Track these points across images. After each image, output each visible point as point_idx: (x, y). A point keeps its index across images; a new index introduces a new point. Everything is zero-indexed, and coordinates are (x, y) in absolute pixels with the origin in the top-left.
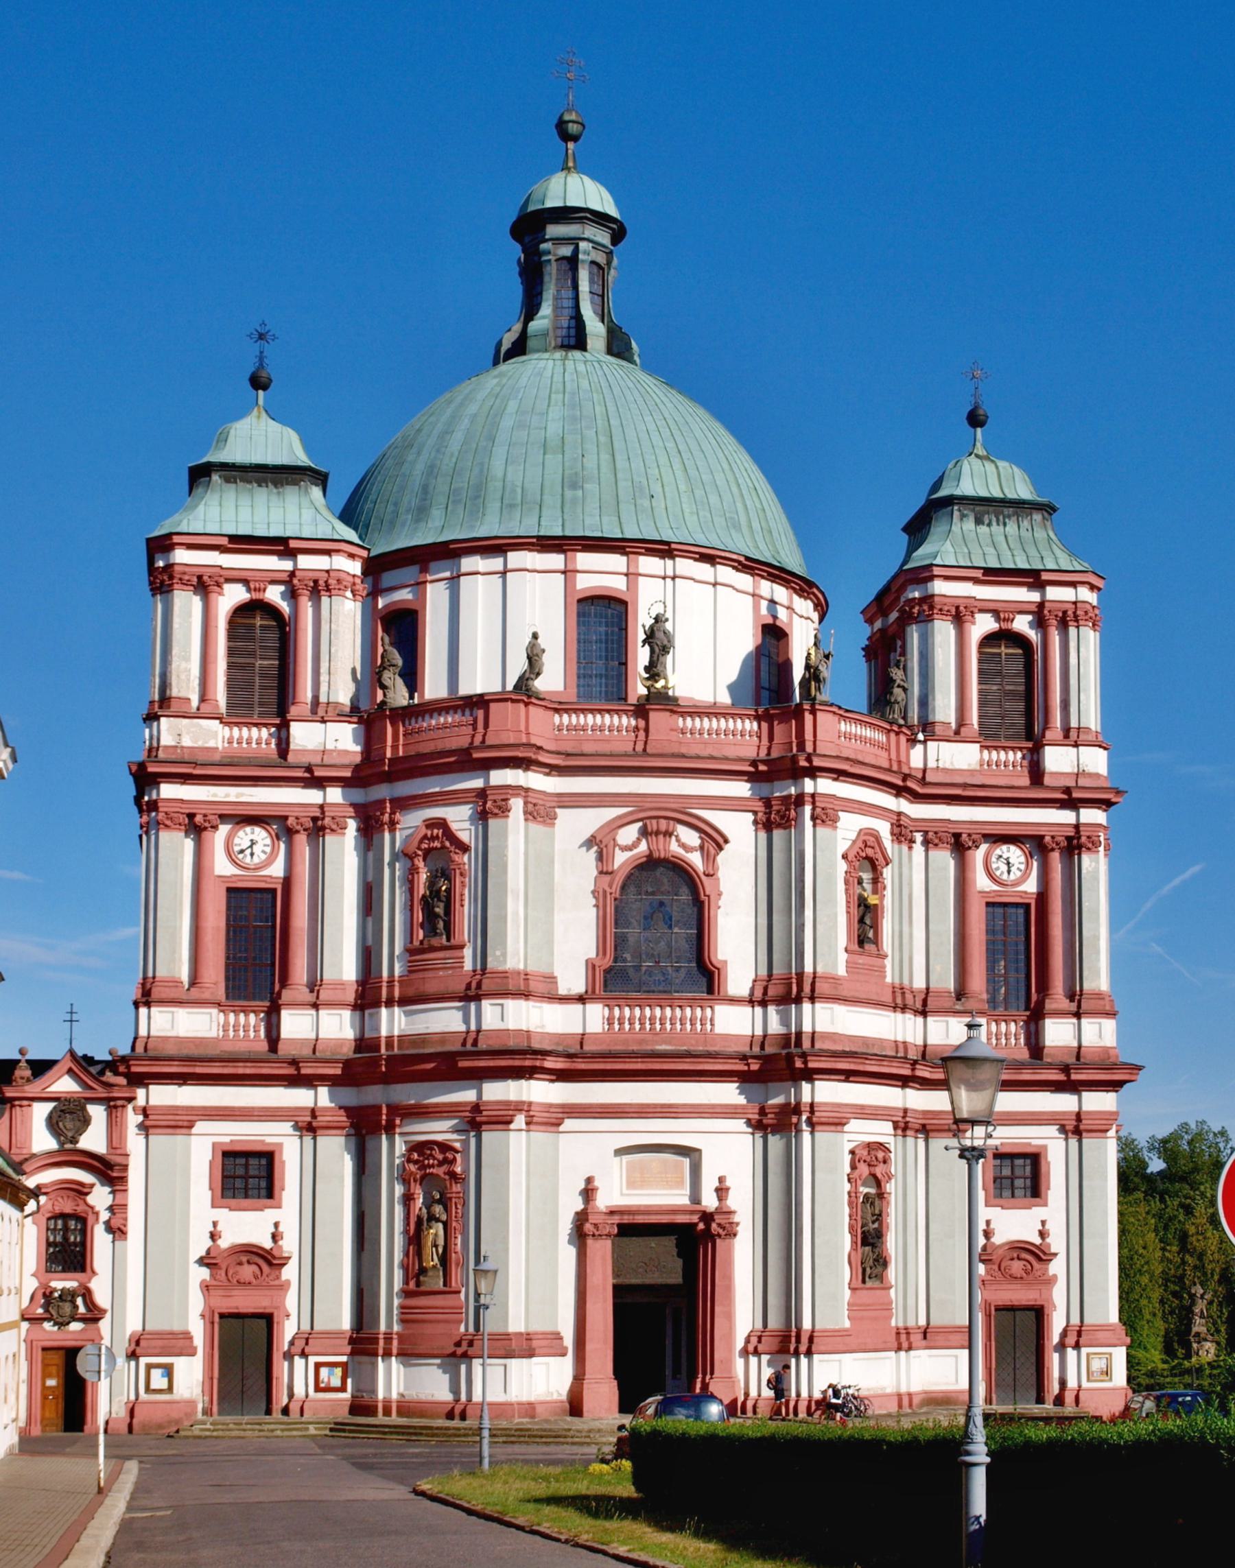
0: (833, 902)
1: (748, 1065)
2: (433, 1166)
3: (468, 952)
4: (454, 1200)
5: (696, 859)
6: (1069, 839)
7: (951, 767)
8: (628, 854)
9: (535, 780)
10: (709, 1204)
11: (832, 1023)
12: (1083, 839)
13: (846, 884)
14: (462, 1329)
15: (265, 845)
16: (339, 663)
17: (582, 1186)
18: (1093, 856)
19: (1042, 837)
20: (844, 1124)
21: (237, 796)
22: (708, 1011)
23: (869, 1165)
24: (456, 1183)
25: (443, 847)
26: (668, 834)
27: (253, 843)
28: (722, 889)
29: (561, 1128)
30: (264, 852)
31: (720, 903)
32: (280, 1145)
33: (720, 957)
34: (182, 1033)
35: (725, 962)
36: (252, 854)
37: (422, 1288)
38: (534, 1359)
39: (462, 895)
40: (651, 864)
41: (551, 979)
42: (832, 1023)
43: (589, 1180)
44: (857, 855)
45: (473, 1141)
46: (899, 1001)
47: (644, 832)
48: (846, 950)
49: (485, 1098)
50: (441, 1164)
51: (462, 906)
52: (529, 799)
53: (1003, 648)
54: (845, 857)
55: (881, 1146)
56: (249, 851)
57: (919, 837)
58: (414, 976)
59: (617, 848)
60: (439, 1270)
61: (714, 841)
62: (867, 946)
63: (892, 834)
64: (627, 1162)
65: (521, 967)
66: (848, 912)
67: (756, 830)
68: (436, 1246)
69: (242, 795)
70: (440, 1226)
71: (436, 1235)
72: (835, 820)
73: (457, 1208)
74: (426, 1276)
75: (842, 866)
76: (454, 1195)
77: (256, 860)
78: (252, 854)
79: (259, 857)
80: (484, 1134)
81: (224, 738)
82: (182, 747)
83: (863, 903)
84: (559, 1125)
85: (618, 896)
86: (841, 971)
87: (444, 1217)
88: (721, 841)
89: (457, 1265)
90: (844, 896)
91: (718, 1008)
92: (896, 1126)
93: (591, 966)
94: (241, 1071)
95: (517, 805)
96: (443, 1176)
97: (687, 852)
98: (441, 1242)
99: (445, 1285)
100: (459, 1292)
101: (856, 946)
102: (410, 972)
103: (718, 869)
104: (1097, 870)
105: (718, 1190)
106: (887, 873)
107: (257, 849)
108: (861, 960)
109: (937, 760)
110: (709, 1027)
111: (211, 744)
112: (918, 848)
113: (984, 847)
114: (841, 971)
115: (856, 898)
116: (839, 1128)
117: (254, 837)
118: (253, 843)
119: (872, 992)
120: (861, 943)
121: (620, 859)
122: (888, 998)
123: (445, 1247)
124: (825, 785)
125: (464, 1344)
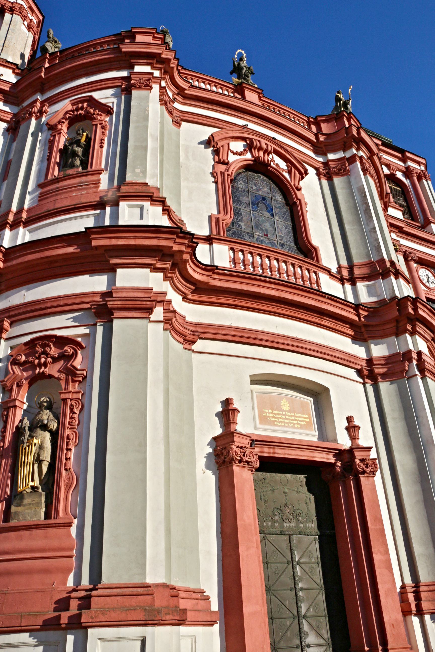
1: (358, 315)
2: (45, 364)
4: (69, 403)
8: (237, 157)
10: (344, 443)
14: (70, 583)
17: (219, 409)
24: (74, 381)
25: (88, 112)
37: (13, 523)
38: (183, 629)
39: (102, 140)
43: (227, 403)
45: (100, 330)
49: (119, 284)
50: (55, 360)
51: (102, 147)
58: (42, 202)
60: (41, 495)
67: (320, 179)
68: (39, 461)
70: (47, 435)
71: (41, 447)
73: (72, 412)
74: (19, 505)
76: (70, 396)
80: (116, 323)
84: (193, 342)
87: (54, 425)
89: (68, 487)
96: (57, 375)
98: (47, 456)
99: (47, 516)
100: (69, 525)
102: (39, 201)
105: (347, 429)
123: (52, 466)
125: (74, 604)
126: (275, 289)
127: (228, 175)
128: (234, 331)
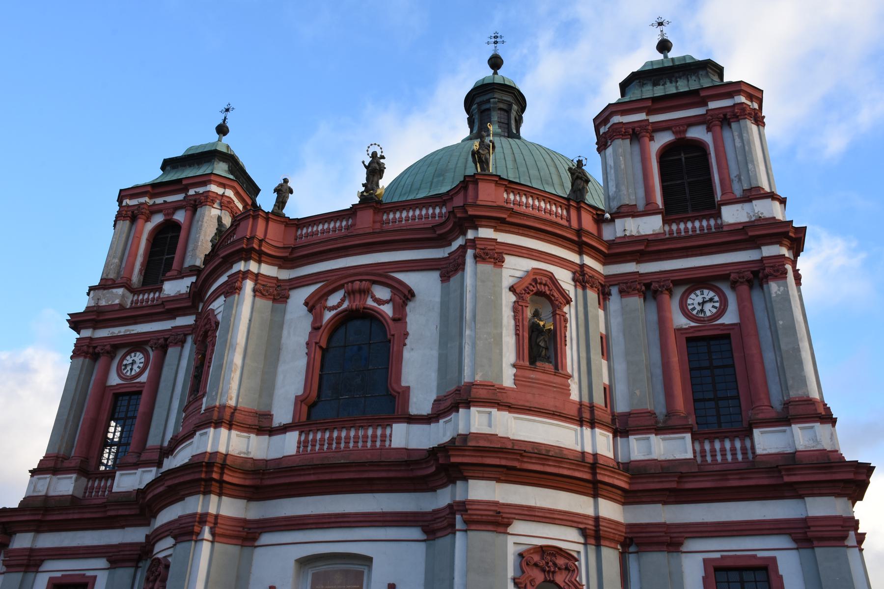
0: (498, 324)
3: (204, 400)
5: (388, 310)
6: (755, 274)
7: (637, 235)
8: (333, 312)
9: (268, 270)
11: (490, 425)
12: (767, 270)
13: (514, 312)
15: (140, 363)
16: (200, 243)
18: (781, 282)
19: (728, 275)
20: (508, 525)
21: (126, 331)
22: (388, 431)
23: (543, 571)
26: (366, 292)
27: (134, 362)
28: (408, 330)
29: (257, 544)
30: (139, 367)
31: (407, 341)
32: (95, 577)
33: (404, 384)
34: (52, 493)
35: (408, 388)
36: (131, 369)
39: (211, 359)
40: (346, 318)
41: (269, 416)
42: (490, 425)
44: (527, 290)
46: (586, 415)
47: (350, 294)
48: (514, 366)
52: (259, 281)
53: (682, 155)
54: (512, 289)
55: (559, 551)
56: (130, 367)
57: (614, 290)
59: (326, 310)
61: (404, 295)
62: (538, 364)
63: (574, 280)
64: (313, 574)
65: (232, 403)
66: (517, 335)
69: (128, 330)
72: (502, 261)
75: (508, 299)
77: (133, 373)
78: (131, 369)
79: (136, 369)
81: (132, 301)
82: (99, 306)
83: (535, 330)
84: (255, 539)
85: (324, 344)
86: (508, 379)
88: (407, 293)
90: (512, 322)
91: (395, 426)
92: (584, 532)
93: (299, 401)
94: (70, 517)
95: (249, 285)
97: (379, 305)
101: (527, 363)
103: (406, 315)
104: (786, 293)
106: (570, 311)
107: (135, 367)
108: (533, 375)
109: (625, 230)
110: (387, 443)
111: (117, 302)
112: (615, 302)
113: (679, 292)
114: (508, 379)
115: (526, 323)
116: (501, 529)
117: (135, 359)
118: (134, 362)
119: (550, 402)
120: (533, 360)
121: (328, 315)
122: (574, 412)
124: (485, 233)
126: (314, 474)
127: (316, 343)
128: (285, 521)
